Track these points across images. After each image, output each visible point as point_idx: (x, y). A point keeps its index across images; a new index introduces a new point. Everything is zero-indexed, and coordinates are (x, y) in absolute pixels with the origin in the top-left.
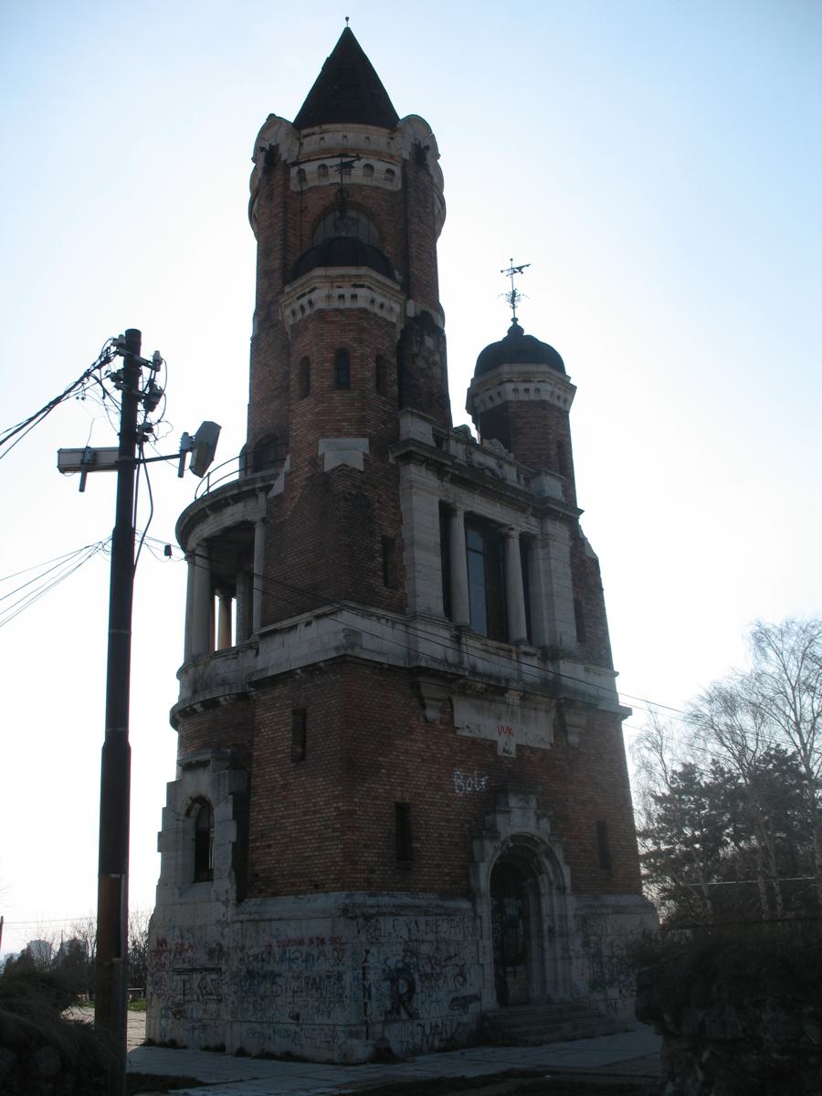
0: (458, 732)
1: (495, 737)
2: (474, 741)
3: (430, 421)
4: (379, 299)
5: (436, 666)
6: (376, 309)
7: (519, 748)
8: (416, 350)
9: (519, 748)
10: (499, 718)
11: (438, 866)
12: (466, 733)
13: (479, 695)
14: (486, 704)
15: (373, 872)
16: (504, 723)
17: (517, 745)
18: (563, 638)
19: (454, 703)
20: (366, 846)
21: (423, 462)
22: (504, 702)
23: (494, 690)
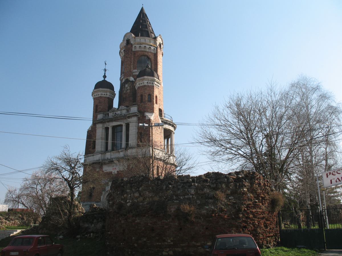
0: (104, 172)
1: (112, 171)
2: (107, 173)
3: (102, 113)
4: (95, 94)
5: (94, 162)
6: (96, 96)
7: (118, 172)
8: (123, 89)
9: (118, 172)
10: (113, 167)
11: (97, 197)
12: (106, 171)
13: (108, 163)
14: (110, 165)
15: (85, 199)
16: (114, 167)
18: (131, 144)
19: (103, 166)
20: (84, 195)
23: (111, 162)
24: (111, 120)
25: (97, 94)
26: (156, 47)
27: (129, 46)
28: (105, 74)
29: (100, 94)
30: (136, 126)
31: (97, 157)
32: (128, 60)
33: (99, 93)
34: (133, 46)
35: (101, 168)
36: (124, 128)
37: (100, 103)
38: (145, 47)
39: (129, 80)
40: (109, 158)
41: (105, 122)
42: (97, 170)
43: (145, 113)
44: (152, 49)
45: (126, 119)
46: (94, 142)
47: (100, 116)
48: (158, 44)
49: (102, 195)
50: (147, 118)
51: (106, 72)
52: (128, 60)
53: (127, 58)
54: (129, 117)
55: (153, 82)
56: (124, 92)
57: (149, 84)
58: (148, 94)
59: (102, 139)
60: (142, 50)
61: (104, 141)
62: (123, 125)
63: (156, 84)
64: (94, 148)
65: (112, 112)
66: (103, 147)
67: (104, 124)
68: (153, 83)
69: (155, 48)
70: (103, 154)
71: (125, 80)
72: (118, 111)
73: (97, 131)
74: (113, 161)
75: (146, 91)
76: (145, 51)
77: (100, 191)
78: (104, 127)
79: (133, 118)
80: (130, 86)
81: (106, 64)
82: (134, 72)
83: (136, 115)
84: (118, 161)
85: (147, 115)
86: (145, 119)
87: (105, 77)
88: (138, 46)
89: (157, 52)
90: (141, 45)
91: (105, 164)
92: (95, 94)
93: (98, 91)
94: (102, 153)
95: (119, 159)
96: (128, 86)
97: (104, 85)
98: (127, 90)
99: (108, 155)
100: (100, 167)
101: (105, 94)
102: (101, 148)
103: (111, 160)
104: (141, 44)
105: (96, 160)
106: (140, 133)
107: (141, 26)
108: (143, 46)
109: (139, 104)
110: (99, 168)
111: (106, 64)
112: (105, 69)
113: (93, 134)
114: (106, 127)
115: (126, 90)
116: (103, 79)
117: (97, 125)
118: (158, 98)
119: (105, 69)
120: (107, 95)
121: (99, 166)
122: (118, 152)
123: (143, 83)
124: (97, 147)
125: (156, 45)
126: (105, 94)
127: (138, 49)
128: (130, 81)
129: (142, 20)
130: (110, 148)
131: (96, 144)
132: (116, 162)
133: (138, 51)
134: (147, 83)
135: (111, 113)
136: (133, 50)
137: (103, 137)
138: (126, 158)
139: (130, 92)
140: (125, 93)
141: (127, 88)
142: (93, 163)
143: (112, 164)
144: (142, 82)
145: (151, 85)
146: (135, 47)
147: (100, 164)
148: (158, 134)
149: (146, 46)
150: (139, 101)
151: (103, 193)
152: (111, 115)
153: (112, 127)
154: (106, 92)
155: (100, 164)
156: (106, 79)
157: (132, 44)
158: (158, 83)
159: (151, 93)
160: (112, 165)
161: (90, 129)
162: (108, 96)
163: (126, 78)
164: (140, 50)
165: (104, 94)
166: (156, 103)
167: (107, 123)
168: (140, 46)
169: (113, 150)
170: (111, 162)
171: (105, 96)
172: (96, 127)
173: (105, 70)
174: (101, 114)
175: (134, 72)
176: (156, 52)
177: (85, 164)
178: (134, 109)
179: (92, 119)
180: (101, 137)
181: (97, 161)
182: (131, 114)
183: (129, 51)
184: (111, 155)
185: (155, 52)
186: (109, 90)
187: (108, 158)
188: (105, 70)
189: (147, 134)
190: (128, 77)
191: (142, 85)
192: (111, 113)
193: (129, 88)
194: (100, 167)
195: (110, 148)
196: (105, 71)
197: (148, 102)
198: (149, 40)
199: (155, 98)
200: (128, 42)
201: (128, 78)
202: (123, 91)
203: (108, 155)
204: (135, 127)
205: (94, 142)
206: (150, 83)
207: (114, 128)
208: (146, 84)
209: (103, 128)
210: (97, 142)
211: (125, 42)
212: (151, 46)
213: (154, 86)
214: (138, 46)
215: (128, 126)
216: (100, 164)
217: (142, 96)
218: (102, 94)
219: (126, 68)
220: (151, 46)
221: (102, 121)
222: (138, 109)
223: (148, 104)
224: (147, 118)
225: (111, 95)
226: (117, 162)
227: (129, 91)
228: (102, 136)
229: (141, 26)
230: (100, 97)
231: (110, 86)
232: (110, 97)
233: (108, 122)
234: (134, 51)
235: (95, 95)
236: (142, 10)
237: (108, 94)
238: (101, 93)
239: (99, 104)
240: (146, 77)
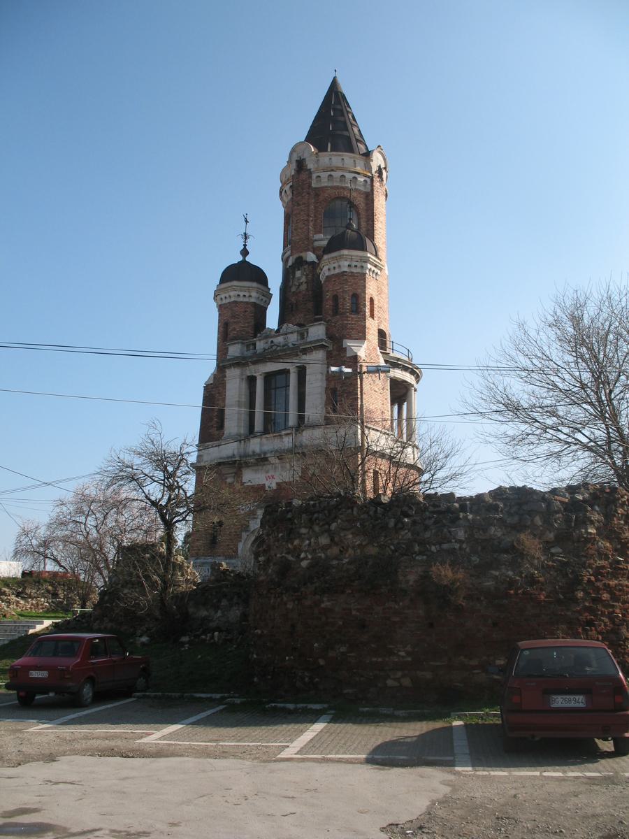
0: (245, 485)
2: (252, 487)
3: (238, 343)
4: (223, 296)
6: (224, 302)
8: (291, 283)
10: (267, 472)
11: (228, 545)
12: (249, 484)
13: (256, 464)
14: (260, 468)
15: (199, 550)
16: (270, 474)
17: (277, 483)
20: (198, 540)
21: (231, 366)
22: (270, 464)
23: (261, 460)
24: (261, 359)
25: (227, 295)
26: (369, 177)
27: (304, 176)
28: (245, 245)
29: (235, 296)
30: (322, 373)
31: (229, 449)
32: (302, 210)
33: (232, 294)
34: (314, 176)
35: (238, 474)
36: (293, 379)
37: (233, 317)
38: (343, 176)
39: (304, 259)
40: (258, 450)
41: (246, 365)
42: (229, 480)
43: (345, 341)
44: (360, 182)
45: (297, 355)
46: (221, 413)
47: (234, 350)
48: (375, 169)
49: (241, 541)
50: (349, 354)
51: (248, 240)
52: (302, 210)
53: (299, 205)
54: (305, 351)
55: (363, 264)
56: (293, 289)
57: (354, 270)
58: (351, 294)
59: (239, 406)
60: (335, 184)
61: (244, 410)
62: (292, 371)
63: (370, 270)
64: (221, 426)
65: (263, 339)
66: (243, 424)
67: (244, 368)
68: (362, 267)
69: (368, 180)
70: (242, 441)
71: (294, 260)
72: (279, 336)
73: (228, 386)
74: (266, 459)
75: (347, 288)
76: (343, 188)
77: (235, 532)
78: (244, 377)
79: (314, 352)
80: (307, 275)
81: (247, 221)
82: (316, 240)
83: (323, 347)
84: (280, 458)
85: (349, 346)
86: (344, 356)
87: (245, 252)
88: (324, 175)
89: (372, 190)
90: (332, 173)
91: (247, 465)
92: (223, 296)
93: (229, 287)
94: (239, 439)
95: (281, 455)
96: (302, 274)
97: (243, 272)
98: (299, 285)
99: (255, 445)
100: (235, 473)
101: (247, 294)
102: (239, 426)
103: (262, 456)
104: (332, 170)
105: (224, 456)
106: (331, 389)
107: (333, 124)
108: (337, 174)
109: (330, 318)
110: (233, 475)
111: (247, 221)
112: (245, 234)
113: (219, 393)
114: (248, 377)
115: (297, 284)
116: (241, 258)
117: (227, 370)
118: (376, 302)
119: (245, 234)
120: (250, 296)
121: (235, 470)
122: (280, 435)
123: (339, 266)
124: (227, 424)
125: (371, 172)
126: (247, 294)
127: (325, 183)
128: (307, 262)
129: (334, 110)
130: (258, 426)
131: (226, 417)
132: (274, 460)
133: (326, 187)
134: (349, 266)
135: (262, 342)
136: (313, 185)
137: (243, 400)
138: (298, 452)
139: (307, 289)
140: (294, 292)
141: (299, 279)
142: (219, 464)
143: (264, 465)
144: (336, 265)
145: (359, 270)
146: (319, 178)
147: (236, 465)
148: (376, 391)
149: (345, 174)
150: (330, 312)
151: (244, 535)
152: (260, 345)
153: (264, 375)
154: (249, 289)
155: (236, 465)
156: (248, 259)
157: (310, 169)
158: (376, 266)
159: (359, 291)
160: (264, 467)
161: (212, 382)
162: (253, 300)
163: (296, 256)
164: (330, 184)
165: (244, 296)
166: (372, 316)
167: (252, 367)
168: (330, 175)
169: (266, 431)
170: (261, 460)
171: (246, 300)
172: (225, 377)
173: (246, 236)
174: (237, 345)
175: (316, 240)
176: (369, 190)
177: (199, 465)
178: (317, 332)
179: (215, 357)
180: (239, 401)
181: (228, 458)
182: (310, 342)
183: (303, 189)
184: (261, 445)
185: (369, 190)
186: (255, 284)
187: (254, 452)
188: (246, 236)
189: (350, 392)
190: (301, 252)
191: (337, 271)
192: (260, 340)
193: (304, 279)
194: (235, 473)
195: (258, 426)
196: (246, 238)
197: (351, 314)
198: (353, 160)
199: (368, 304)
200: (300, 165)
201: (302, 254)
202: (291, 287)
203: (255, 445)
204: (319, 376)
205: (222, 412)
206: (356, 266)
207: (268, 377)
208: (346, 269)
209: (243, 379)
210: (228, 411)
211: (294, 165)
212: (356, 176)
213: (365, 274)
214: (324, 175)
215: (302, 372)
216: (236, 465)
217: (335, 298)
218: (239, 295)
219: (296, 230)
220: (359, 173)
221: (240, 363)
222: (327, 329)
223: (352, 318)
224: (349, 354)
225: (261, 297)
226: (277, 461)
227: (304, 287)
228: (239, 398)
229: (333, 124)
230: (235, 302)
231: (259, 276)
232: (258, 302)
233: (254, 363)
234: (315, 188)
235: (221, 299)
236: (334, 84)
237: (254, 294)
238: (237, 293)
239: (232, 320)
240: (345, 252)
